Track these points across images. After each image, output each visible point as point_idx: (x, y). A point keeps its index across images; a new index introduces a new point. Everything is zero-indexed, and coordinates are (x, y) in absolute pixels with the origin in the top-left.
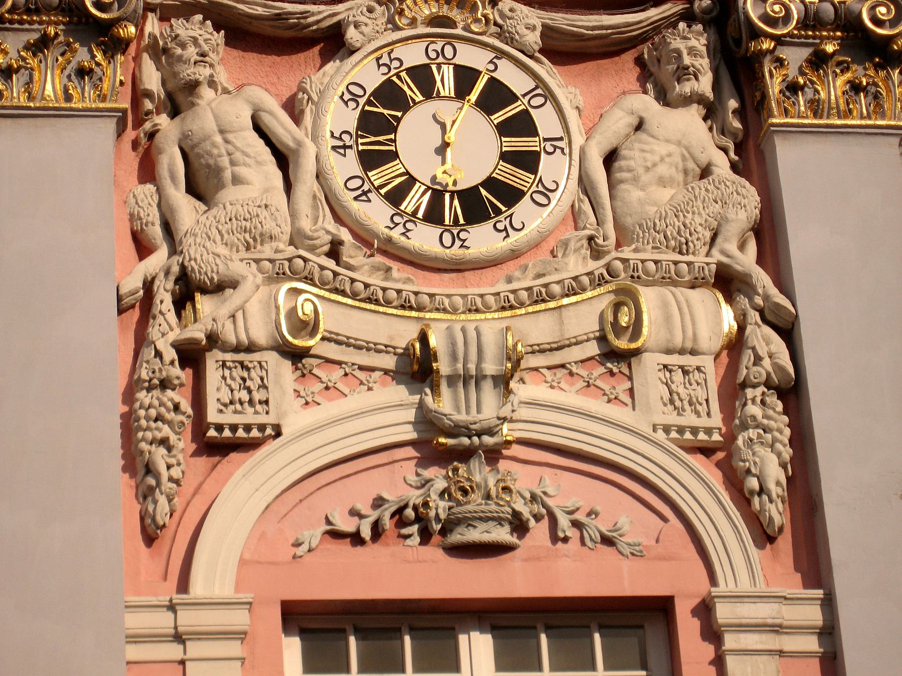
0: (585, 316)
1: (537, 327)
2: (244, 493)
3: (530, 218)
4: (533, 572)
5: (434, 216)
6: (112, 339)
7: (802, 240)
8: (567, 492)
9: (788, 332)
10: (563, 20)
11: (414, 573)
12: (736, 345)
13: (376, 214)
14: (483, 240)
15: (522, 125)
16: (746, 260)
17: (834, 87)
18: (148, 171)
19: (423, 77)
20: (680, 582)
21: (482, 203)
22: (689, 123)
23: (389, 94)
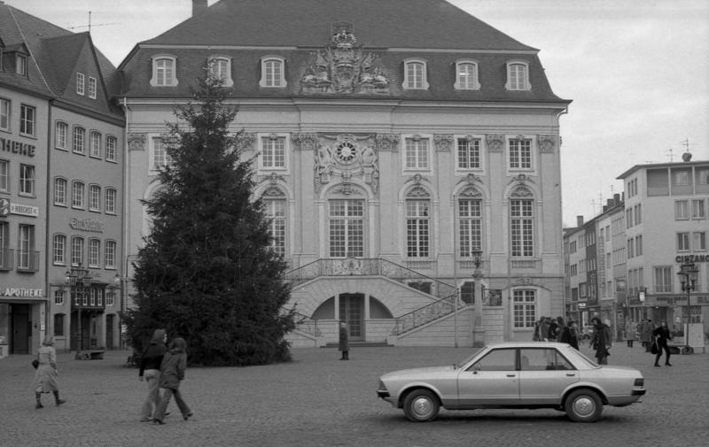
0: (359, 170)
1: (353, 172)
2: (326, 187)
3: (354, 159)
4: (352, 197)
5: (344, 159)
6: (312, 172)
7: (381, 162)
8: (355, 188)
9: (378, 172)
10: (359, 138)
11: (340, 196)
12: (373, 172)
13: (339, 160)
14: (349, 162)
15: (354, 150)
16: (375, 165)
17: (385, 146)
18: (317, 155)
19: (344, 144)
20: (366, 198)
21: (350, 158)
22: (371, 150)
23: (341, 146)
